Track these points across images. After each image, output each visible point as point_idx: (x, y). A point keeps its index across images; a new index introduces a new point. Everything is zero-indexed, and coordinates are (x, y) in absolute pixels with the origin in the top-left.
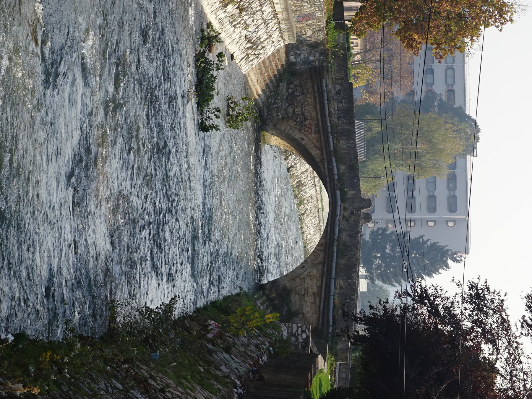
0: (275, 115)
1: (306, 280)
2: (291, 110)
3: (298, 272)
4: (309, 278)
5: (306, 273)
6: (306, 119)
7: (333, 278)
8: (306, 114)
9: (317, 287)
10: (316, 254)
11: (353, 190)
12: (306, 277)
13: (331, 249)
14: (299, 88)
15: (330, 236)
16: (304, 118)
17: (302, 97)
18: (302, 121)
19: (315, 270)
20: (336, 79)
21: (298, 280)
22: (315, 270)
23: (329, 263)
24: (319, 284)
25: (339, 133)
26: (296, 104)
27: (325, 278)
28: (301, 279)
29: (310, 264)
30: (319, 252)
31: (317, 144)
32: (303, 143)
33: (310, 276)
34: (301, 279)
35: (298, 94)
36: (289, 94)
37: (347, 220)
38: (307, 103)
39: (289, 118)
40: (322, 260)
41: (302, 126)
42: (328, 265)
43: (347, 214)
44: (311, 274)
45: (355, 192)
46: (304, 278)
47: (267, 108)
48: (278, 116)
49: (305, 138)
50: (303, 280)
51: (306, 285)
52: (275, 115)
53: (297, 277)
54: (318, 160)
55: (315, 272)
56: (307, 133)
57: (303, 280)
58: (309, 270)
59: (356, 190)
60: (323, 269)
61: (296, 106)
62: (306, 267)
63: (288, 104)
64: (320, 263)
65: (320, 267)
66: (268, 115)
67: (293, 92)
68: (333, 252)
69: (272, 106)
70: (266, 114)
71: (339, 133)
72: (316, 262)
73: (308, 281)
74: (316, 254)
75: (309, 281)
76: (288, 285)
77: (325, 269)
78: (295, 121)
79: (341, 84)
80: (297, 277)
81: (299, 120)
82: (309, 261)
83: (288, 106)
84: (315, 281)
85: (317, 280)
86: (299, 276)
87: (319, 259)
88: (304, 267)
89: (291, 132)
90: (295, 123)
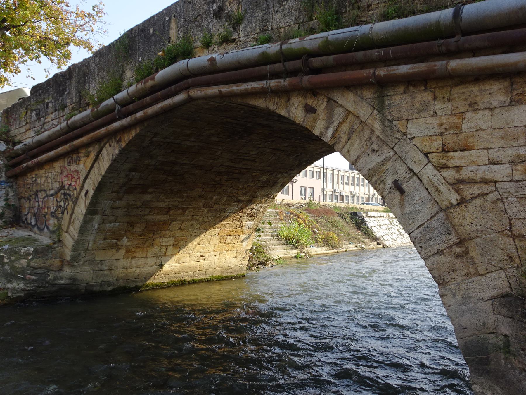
0: (24, 262)
1: (465, 173)
2: (52, 222)
3: (423, 215)
4: (456, 158)
5: (429, 171)
6: (62, 187)
7: (457, 14)
8: (57, 185)
9: (513, 103)
10: (345, 127)
11: (169, 29)
12: (450, 174)
13: (316, 62)
14: (32, 202)
15: (275, 75)
16: (61, 189)
17: (40, 195)
18: (65, 194)
19: (412, 129)
20: (27, 123)
21: (469, 219)
22: (412, 129)
23: (377, 53)
24: (495, 93)
25: (80, 100)
26: (46, 210)
27: (454, 64)
28: (462, 202)
29: (387, 153)
30: (337, 119)
31: (92, 156)
32: (91, 192)
33: (445, 150)
34: (462, 202)
35: (37, 204)
36: (36, 224)
37: (236, 23)
38: (46, 184)
39: (59, 227)
40: (369, 94)
41: (69, 195)
42: (385, 61)
43: (217, 28)
44: (438, 143)
45: (173, 25)
46: (457, 185)
47: (9, 282)
48: (28, 254)
49: (86, 187)
50: (469, 191)
51: (502, 172)
52: (24, 262)
53: (450, 227)
54: (117, 152)
55: (424, 119)
56: (78, 180)
57: (469, 191)
58: (414, 158)
59: (169, 22)
60: (410, 82)
61: (48, 208)
62: (402, 172)
63: (46, 229)
64: (380, 106)
65: (399, 101)
66: (24, 279)
67: (35, 215)
68: (327, 49)
69: (7, 267)
70: (22, 286)
71: (80, 100)
72: (377, 126)
73: (473, 163)
74: (345, 127)
75: (481, 156)
76: (497, 282)
77: (404, 69)
78: (63, 213)
79: (32, 111)
80: (450, 227)
81: (62, 204)
82: (375, 160)
83: (48, 228)
84: (471, 121)
85: (473, 106)
86: (446, 210)
87: (364, 111)
88: (398, 186)
89: (78, 224)
90: (66, 211)
